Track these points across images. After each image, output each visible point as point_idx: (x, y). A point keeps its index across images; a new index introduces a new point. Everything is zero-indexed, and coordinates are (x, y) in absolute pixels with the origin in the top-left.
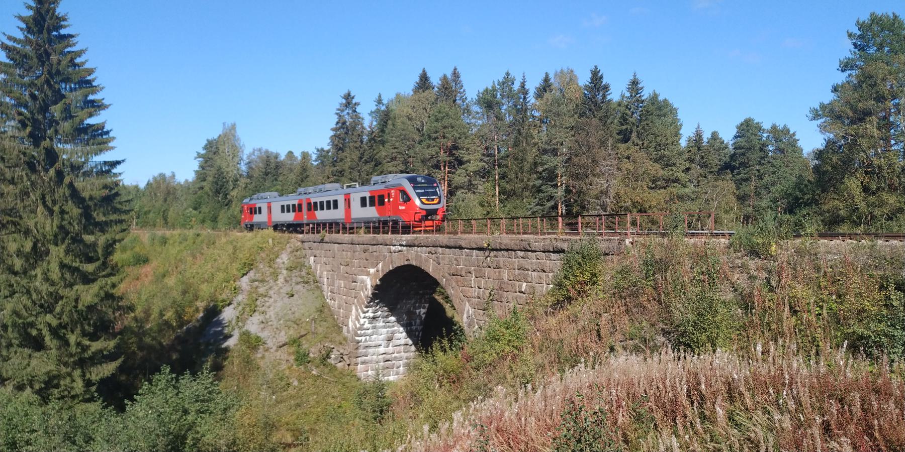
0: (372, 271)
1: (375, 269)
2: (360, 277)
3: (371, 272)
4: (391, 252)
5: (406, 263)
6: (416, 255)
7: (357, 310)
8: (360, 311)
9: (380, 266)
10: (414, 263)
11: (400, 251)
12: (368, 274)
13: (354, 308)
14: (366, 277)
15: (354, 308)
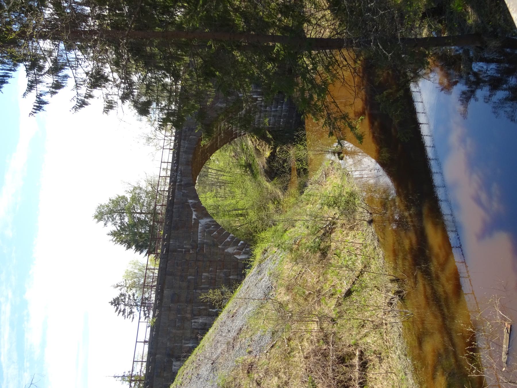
0: (194, 217)
1: (193, 209)
2: (199, 239)
3: (195, 217)
4: (180, 185)
5: (190, 168)
6: (185, 152)
7: (228, 245)
8: (228, 239)
9: (190, 201)
10: (191, 156)
11: (181, 172)
12: (197, 223)
13: (226, 251)
14: (200, 225)
15: (226, 251)
